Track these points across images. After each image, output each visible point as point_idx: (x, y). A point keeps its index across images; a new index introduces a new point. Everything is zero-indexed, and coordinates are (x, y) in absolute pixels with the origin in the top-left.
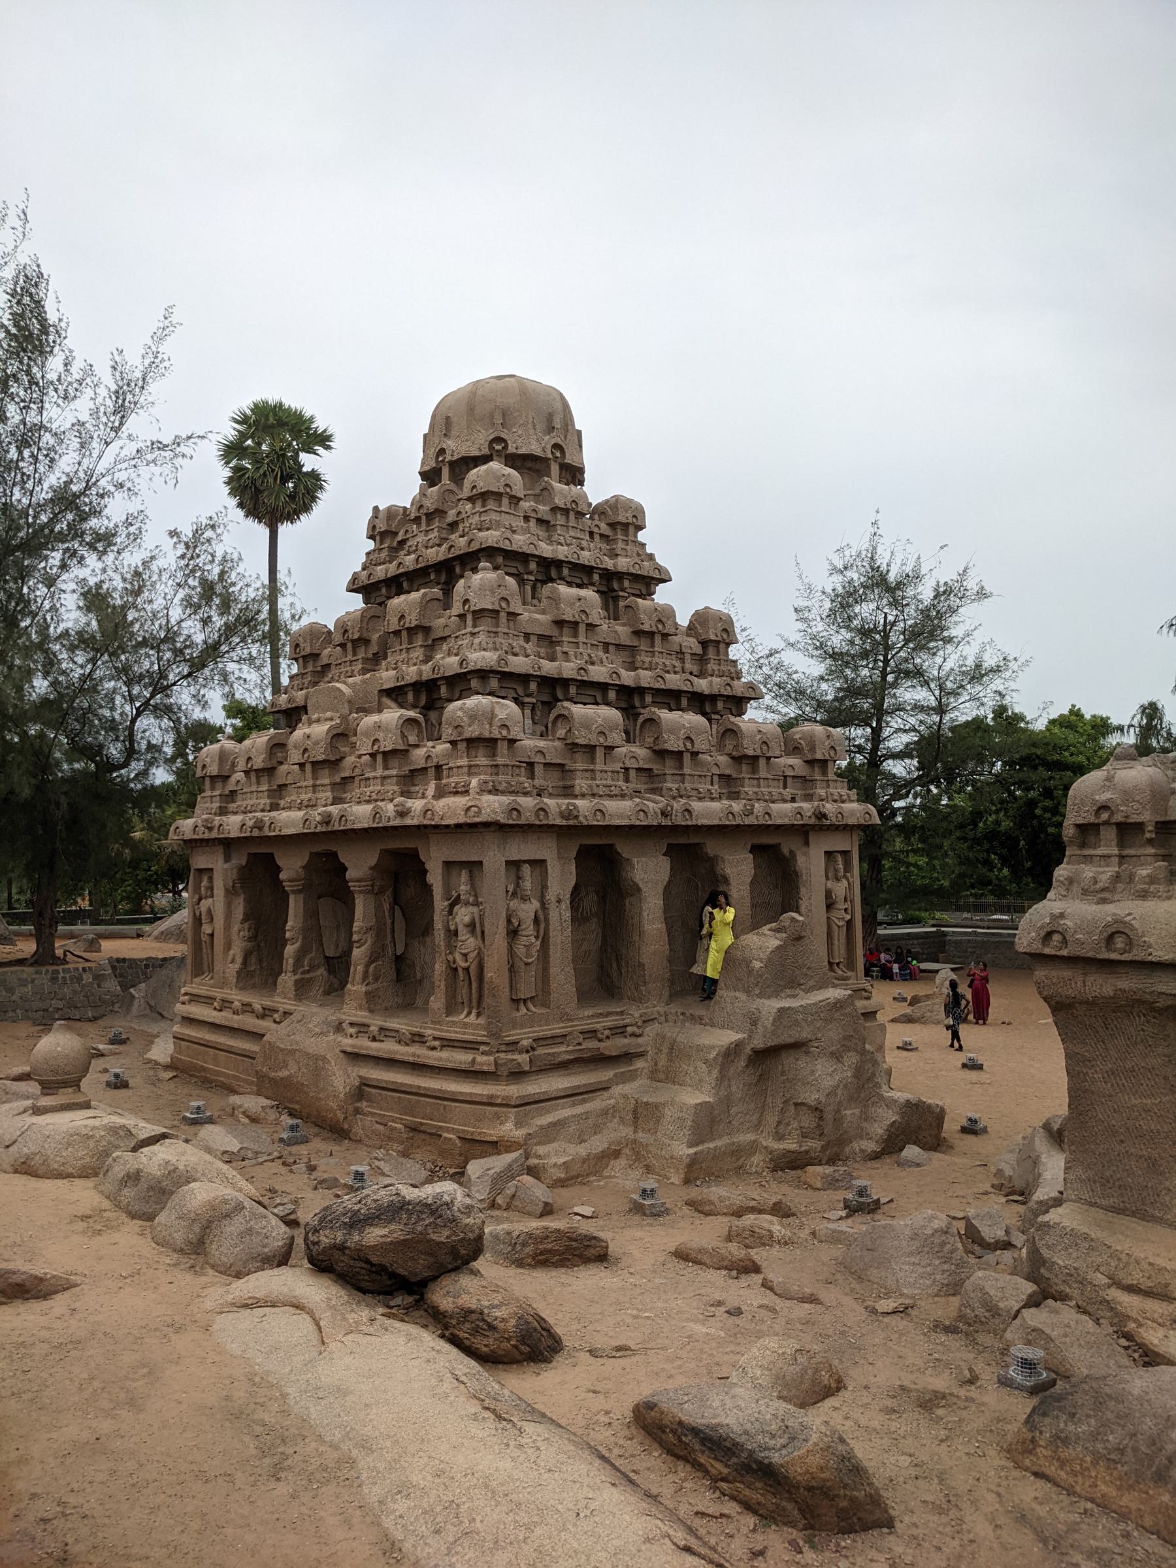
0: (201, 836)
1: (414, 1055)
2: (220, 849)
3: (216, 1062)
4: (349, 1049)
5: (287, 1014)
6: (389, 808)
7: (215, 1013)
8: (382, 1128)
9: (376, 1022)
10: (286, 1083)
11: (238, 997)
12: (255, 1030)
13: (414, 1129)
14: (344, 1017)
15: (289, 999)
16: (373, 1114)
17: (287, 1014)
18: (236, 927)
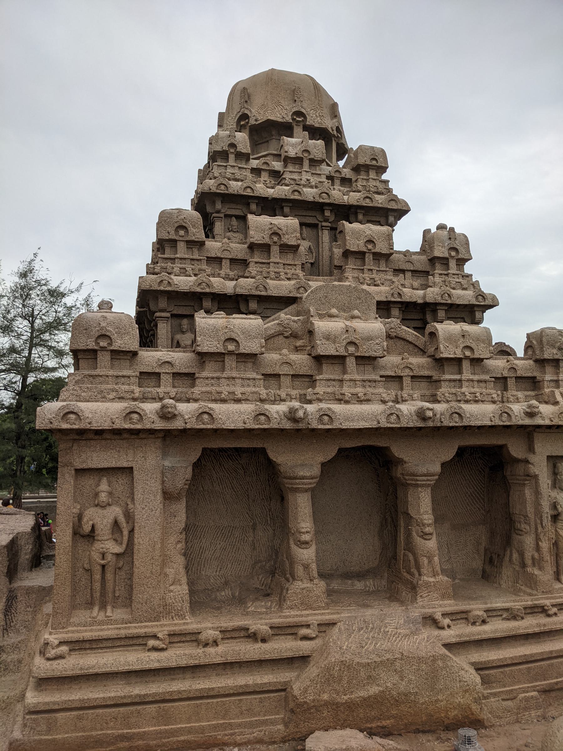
0: (148, 426)
1: (539, 625)
2: (159, 443)
3: (165, 718)
4: (454, 640)
5: (326, 626)
6: (517, 408)
7: (154, 655)
8: (509, 703)
9: (477, 608)
11: (208, 625)
13: (545, 691)
14: (429, 611)
15: (319, 608)
16: (495, 695)
17: (326, 626)
18: (172, 539)
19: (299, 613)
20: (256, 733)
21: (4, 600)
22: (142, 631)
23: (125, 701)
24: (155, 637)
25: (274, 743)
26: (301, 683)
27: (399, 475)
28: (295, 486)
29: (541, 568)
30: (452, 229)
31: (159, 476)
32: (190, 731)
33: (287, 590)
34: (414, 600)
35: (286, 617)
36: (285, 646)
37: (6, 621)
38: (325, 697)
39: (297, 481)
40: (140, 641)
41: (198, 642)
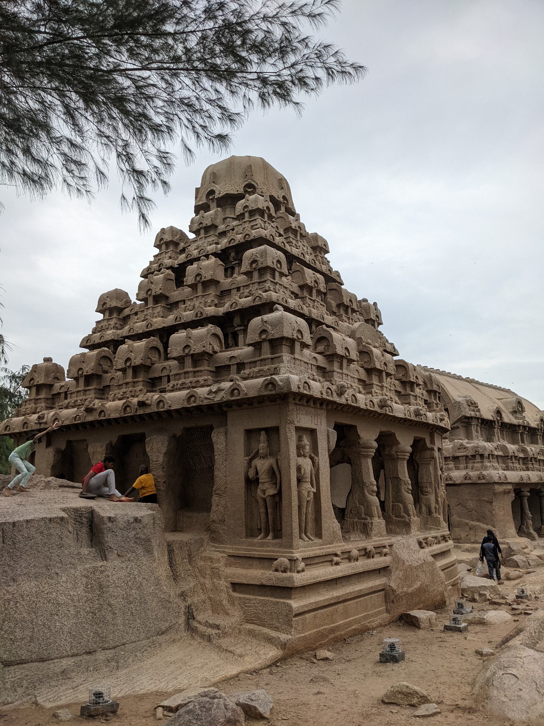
3: (346, 614)
5: (391, 546)
7: (338, 567)
10: (421, 590)
12: (377, 567)
19: (378, 539)
20: (378, 620)
21: (167, 553)
22: (330, 550)
23: (333, 602)
24: (336, 555)
25: (386, 625)
26: (393, 582)
27: (393, 453)
28: (369, 454)
29: (439, 514)
30: (375, 304)
31: (326, 437)
32: (356, 621)
33: (372, 523)
34: (408, 532)
35: (375, 541)
36: (378, 561)
37: (172, 571)
38: (405, 589)
39: (371, 450)
40: (329, 558)
41: (350, 559)
